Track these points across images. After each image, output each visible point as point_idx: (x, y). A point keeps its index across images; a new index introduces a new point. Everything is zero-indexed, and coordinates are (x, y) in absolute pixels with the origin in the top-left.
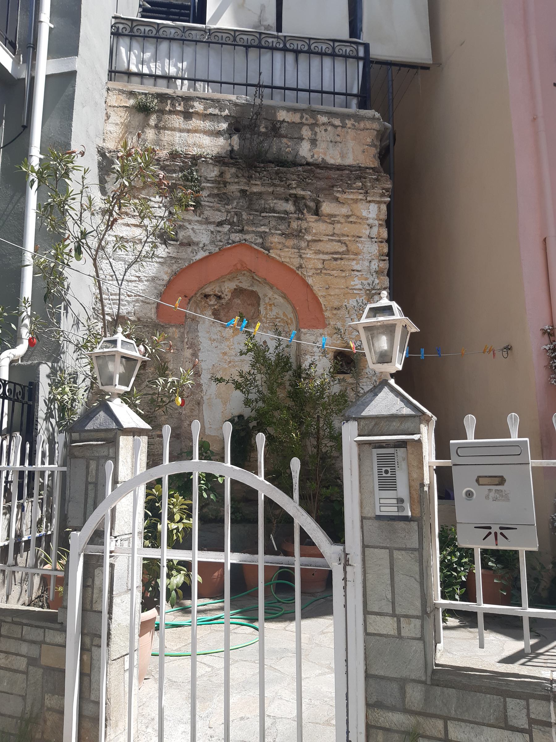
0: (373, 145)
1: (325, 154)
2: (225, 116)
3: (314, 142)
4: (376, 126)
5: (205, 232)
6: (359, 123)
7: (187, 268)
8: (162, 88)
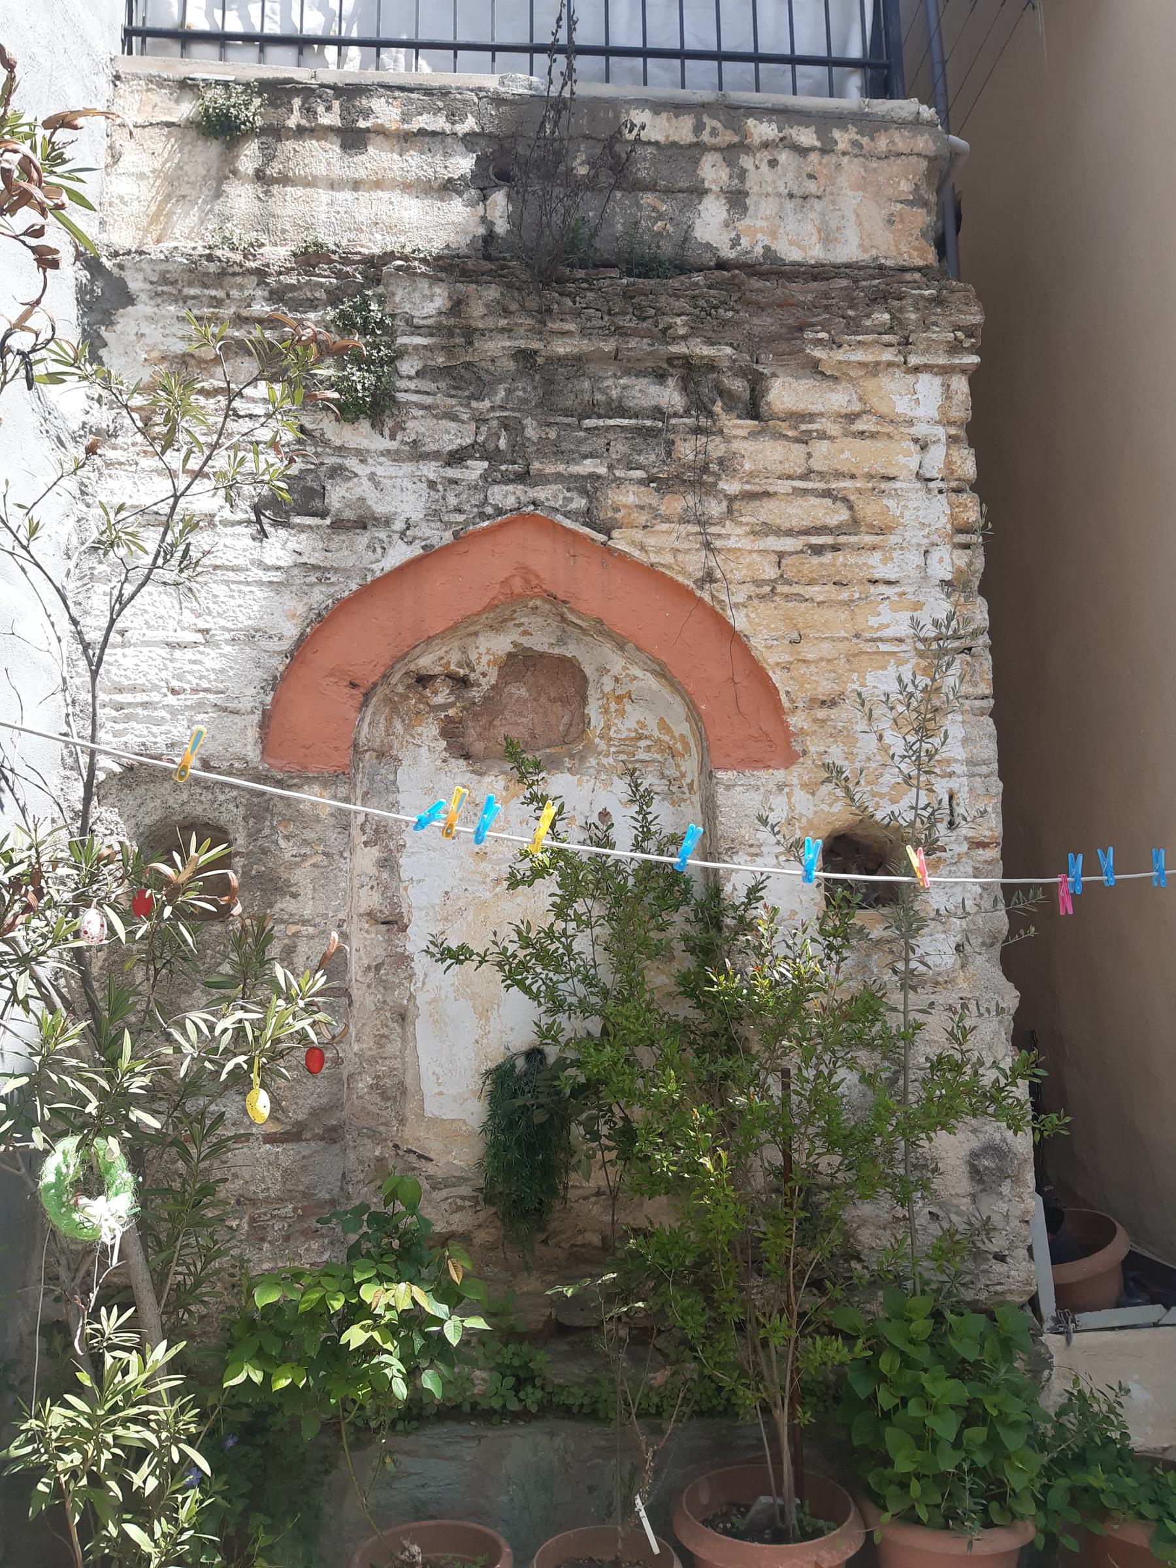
0: (918, 201)
1: (773, 234)
2: (466, 135)
3: (737, 199)
4: (924, 143)
5: (410, 485)
6: (872, 139)
7: (357, 596)
8: (281, 65)
